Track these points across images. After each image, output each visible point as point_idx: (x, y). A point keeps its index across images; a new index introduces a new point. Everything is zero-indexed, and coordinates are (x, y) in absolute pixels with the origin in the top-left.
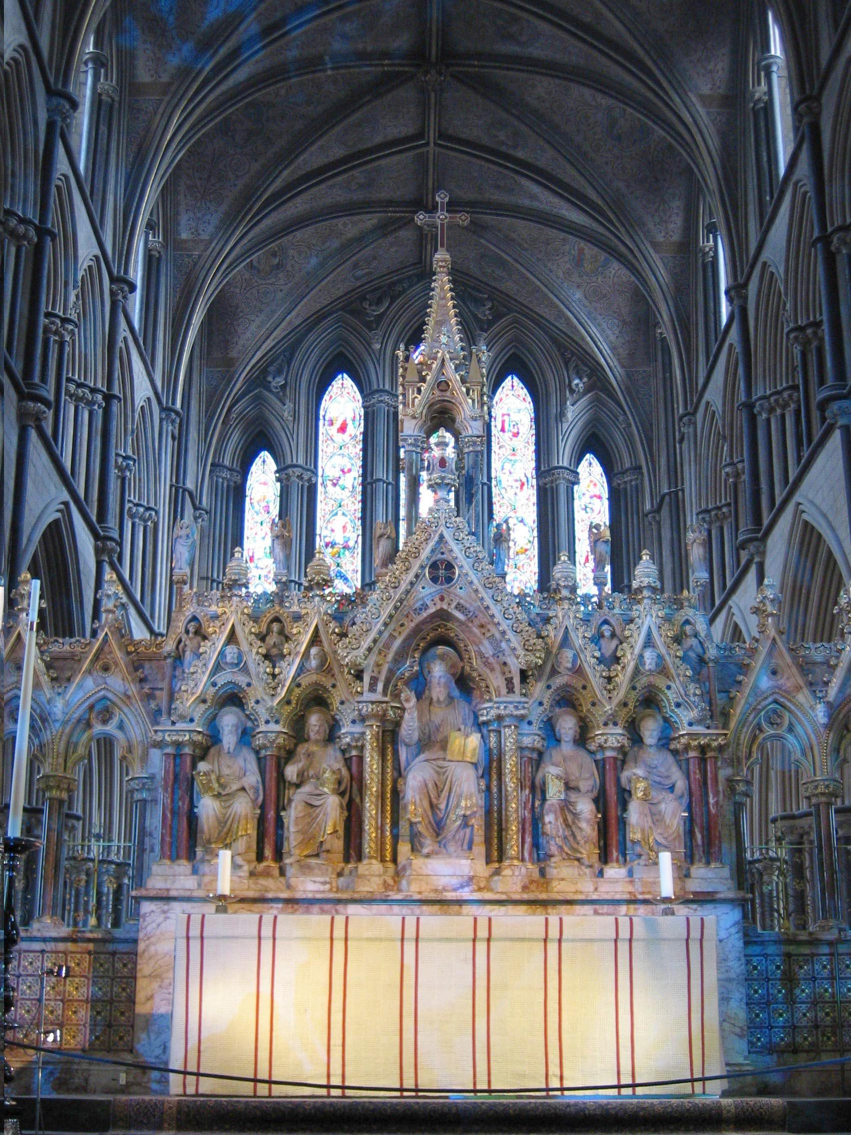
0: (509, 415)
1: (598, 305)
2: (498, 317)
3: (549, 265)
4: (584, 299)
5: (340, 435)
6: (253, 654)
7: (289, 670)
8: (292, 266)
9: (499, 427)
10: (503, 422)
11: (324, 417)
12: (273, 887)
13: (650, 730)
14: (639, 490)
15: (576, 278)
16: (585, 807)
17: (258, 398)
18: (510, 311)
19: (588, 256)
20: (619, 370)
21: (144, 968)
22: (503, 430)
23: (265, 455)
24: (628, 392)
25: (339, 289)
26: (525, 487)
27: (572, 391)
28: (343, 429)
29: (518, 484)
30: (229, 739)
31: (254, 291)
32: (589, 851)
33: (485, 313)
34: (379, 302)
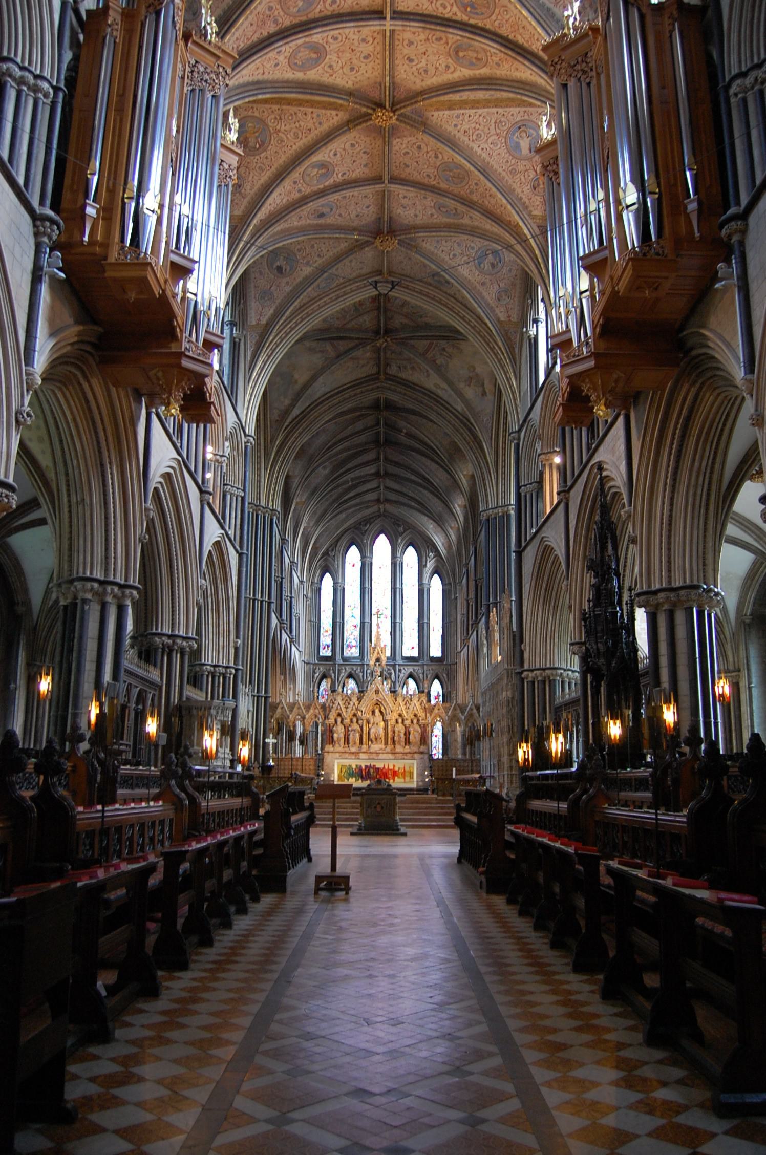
2: (405, 530)
6: (342, 707)
7: (349, 710)
12: (347, 750)
13: (415, 721)
14: (450, 590)
16: (402, 735)
17: (326, 560)
20: (445, 551)
21: (325, 764)
23: (328, 575)
24: (447, 559)
30: (339, 722)
32: (403, 744)
33: (401, 529)
34: (365, 525)
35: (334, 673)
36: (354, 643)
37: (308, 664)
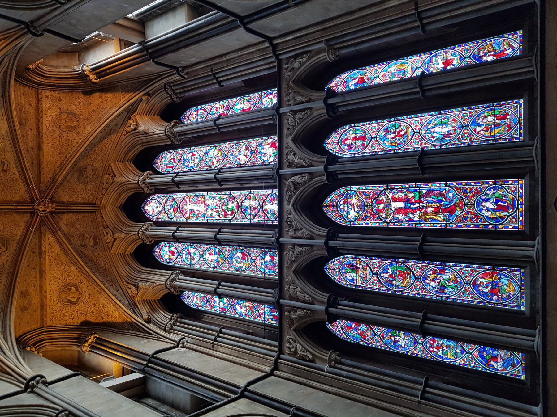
0: (167, 164)
1: (94, 117)
3: (74, 144)
4: (91, 125)
5: (175, 254)
8: (76, 280)
9: (171, 169)
10: (170, 167)
11: (169, 263)
15: (80, 130)
18: (110, 166)
19: (69, 124)
22: (172, 167)
25: (99, 254)
26: (194, 153)
27: (136, 129)
28: (172, 253)
29: (193, 157)
31: (89, 301)
35: (295, 309)
36: (267, 258)
37: (276, 367)
